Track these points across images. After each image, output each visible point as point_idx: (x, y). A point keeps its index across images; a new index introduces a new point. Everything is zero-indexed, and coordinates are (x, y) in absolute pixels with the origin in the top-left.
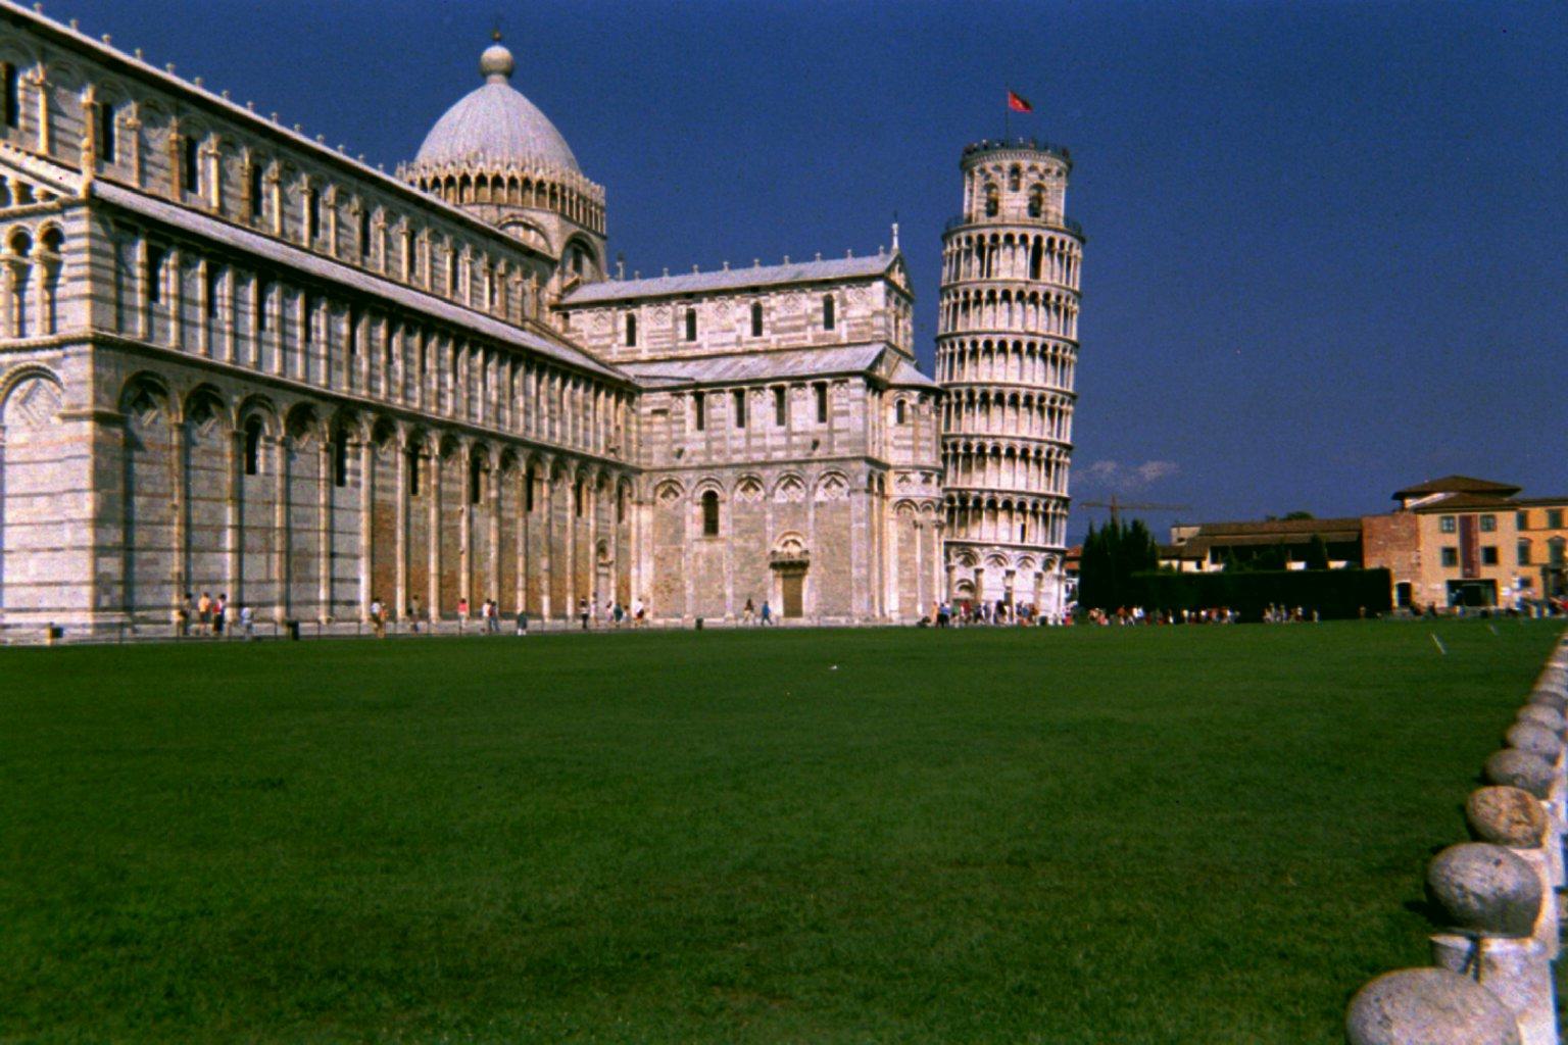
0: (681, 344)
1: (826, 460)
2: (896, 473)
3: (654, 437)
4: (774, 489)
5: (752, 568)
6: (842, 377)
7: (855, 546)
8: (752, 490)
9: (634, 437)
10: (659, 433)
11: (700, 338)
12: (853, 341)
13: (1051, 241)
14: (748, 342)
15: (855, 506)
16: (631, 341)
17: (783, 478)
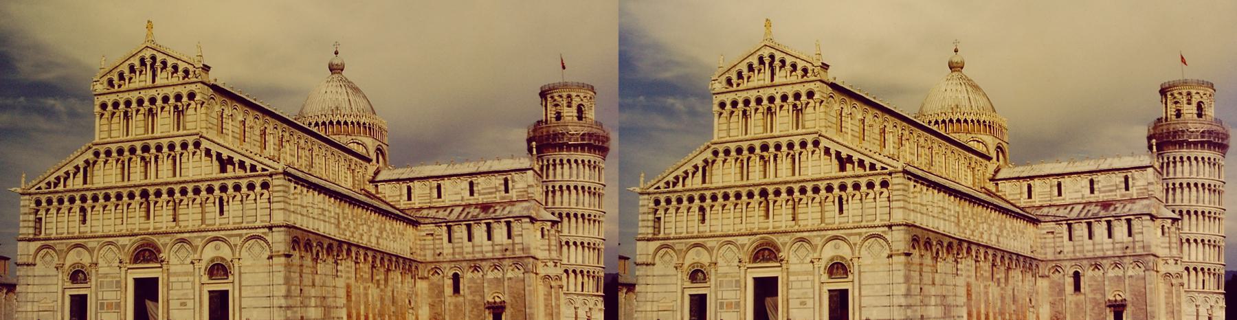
0: (434, 200)
1: (515, 258)
3: (427, 247)
4: (487, 271)
6: (518, 218)
7: (527, 298)
8: (476, 272)
9: (418, 247)
10: (428, 245)
14: (467, 200)
15: (526, 280)
16: (409, 198)
17: (491, 266)
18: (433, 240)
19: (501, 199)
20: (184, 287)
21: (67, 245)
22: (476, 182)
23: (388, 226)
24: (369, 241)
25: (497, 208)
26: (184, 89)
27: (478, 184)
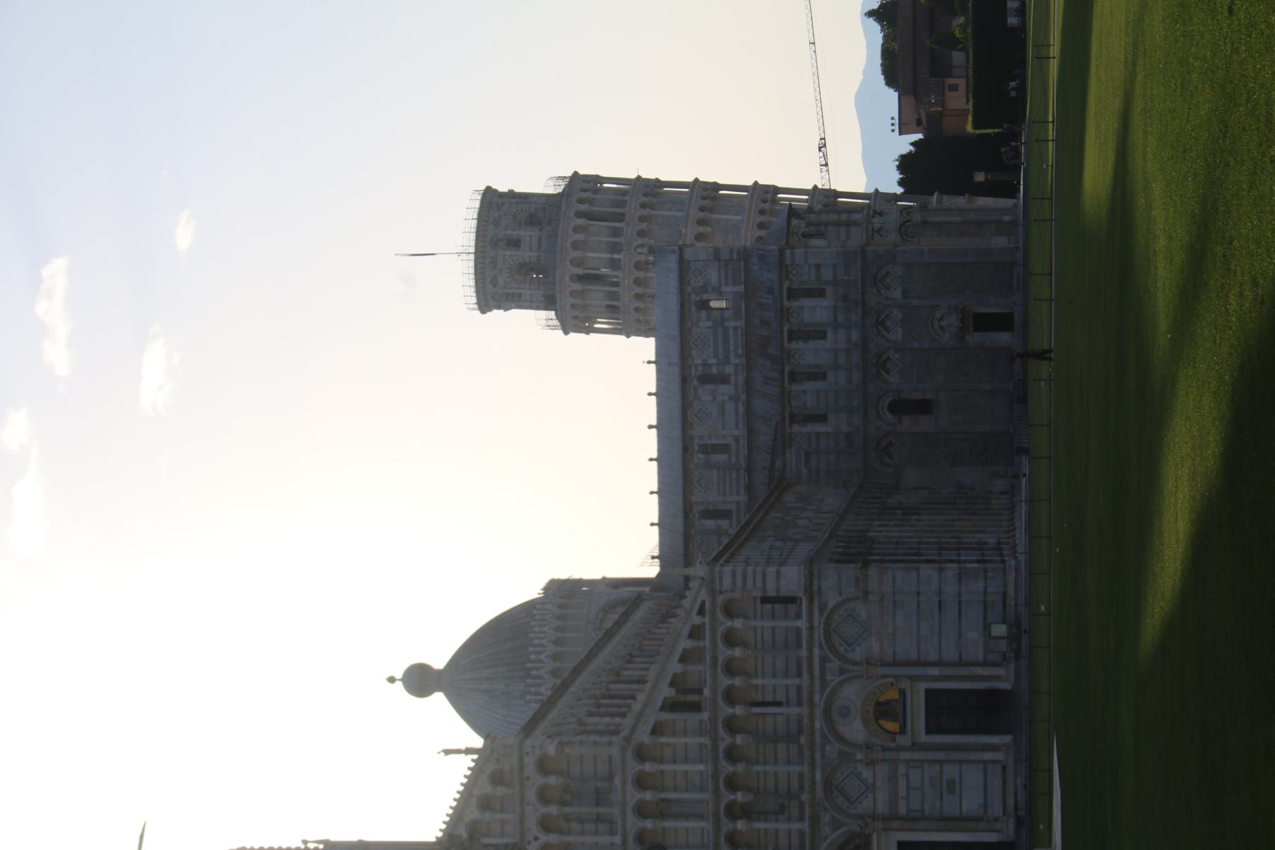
0: (733, 459)
2: (873, 238)
11: (729, 441)
12: (743, 280)
13: (580, 201)
22: (700, 368)
27: (705, 364)
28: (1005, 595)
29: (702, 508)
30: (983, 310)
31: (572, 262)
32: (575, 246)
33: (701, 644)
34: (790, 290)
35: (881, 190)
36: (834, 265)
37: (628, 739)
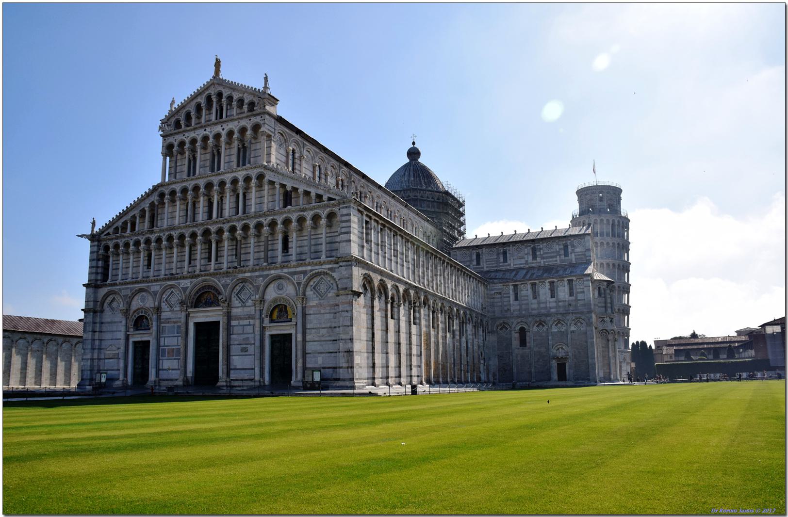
0: (501, 264)
2: (600, 318)
3: (495, 304)
4: (552, 325)
5: (543, 360)
8: (541, 326)
14: (530, 263)
16: (478, 263)
17: (556, 321)
18: (501, 298)
19: (560, 262)
20: (245, 332)
21: (131, 291)
22: (539, 247)
23: (462, 281)
24: (445, 293)
25: (559, 269)
26: (249, 122)
27: (540, 249)
28: (339, 379)
29: (480, 253)
30: (567, 367)
31: (596, 220)
32: (602, 220)
33: (313, 201)
34: (572, 280)
35: (630, 331)
36: (584, 299)
37: (265, 167)
